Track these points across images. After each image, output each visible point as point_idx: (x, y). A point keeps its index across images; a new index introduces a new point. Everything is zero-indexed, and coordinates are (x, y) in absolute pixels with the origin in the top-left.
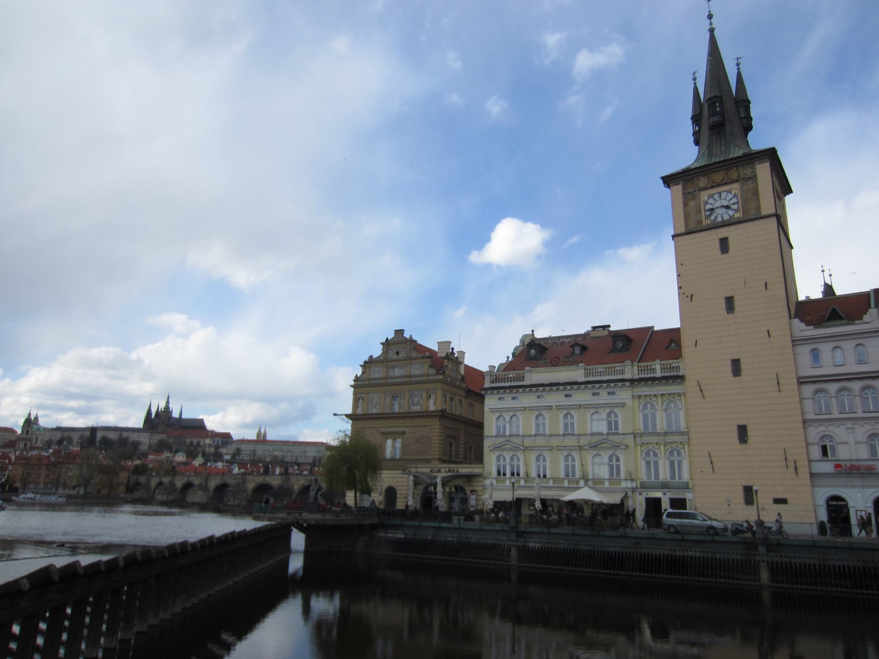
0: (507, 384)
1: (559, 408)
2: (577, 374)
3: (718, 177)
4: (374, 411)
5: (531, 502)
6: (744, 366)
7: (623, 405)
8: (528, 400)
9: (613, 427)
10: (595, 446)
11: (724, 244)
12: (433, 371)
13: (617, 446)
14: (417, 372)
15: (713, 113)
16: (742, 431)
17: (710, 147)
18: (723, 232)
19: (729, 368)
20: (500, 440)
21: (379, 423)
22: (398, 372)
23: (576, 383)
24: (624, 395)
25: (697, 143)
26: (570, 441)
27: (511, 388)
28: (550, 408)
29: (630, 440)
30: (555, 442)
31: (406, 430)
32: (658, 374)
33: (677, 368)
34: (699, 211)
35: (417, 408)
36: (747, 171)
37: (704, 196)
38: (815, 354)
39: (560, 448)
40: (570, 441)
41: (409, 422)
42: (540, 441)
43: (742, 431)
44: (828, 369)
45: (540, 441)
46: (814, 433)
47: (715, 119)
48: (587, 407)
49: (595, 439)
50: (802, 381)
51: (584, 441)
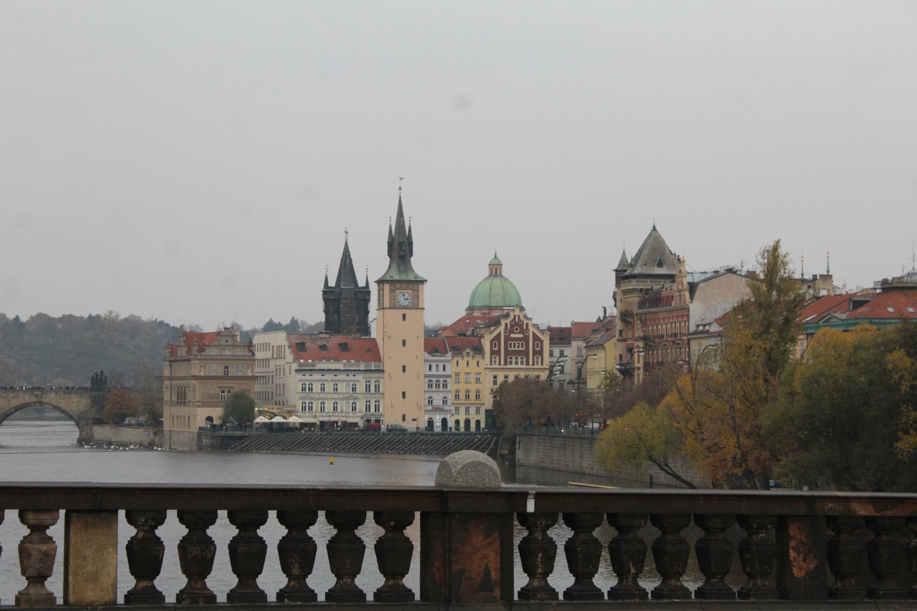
0: (307, 368)
1: (332, 381)
2: (339, 366)
3: (404, 285)
4: (213, 374)
5: (337, 422)
6: (407, 369)
7: (358, 381)
8: (317, 376)
9: (354, 389)
10: (347, 398)
11: (404, 316)
12: (250, 354)
13: (356, 398)
14: (240, 354)
15: (400, 249)
16: (404, 394)
17: (398, 265)
18: (404, 311)
19: (401, 369)
20: (304, 395)
21: (216, 381)
22: (227, 352)
23: (339, 370)
24: (359, 377)
25: (390, 255)
26: (336, 396)
27: (311, 370)
28: (327, 380)
29: (361, 396)
30: (329, 396)
31: (235, 386)
32: (373, 368)
33: (379, 366)
34: (395, 299)
35: (241, 374)
36: (415, 286)
37: (398, 292)
38: (430, 366)
39: (332, 399)
40: (336, 396)
41: (236, 381)
42: (323, 396)
43: (404, 394)
44: (434, 372)
45: (323, 396)
46: (428, 395)
47: (401, 253)
48: (344, 381)
49: (346, 395)
50: (426, 376)
51: (342, 396)
